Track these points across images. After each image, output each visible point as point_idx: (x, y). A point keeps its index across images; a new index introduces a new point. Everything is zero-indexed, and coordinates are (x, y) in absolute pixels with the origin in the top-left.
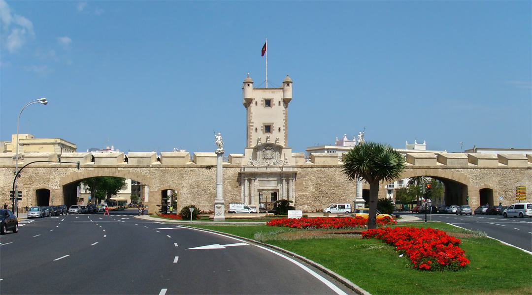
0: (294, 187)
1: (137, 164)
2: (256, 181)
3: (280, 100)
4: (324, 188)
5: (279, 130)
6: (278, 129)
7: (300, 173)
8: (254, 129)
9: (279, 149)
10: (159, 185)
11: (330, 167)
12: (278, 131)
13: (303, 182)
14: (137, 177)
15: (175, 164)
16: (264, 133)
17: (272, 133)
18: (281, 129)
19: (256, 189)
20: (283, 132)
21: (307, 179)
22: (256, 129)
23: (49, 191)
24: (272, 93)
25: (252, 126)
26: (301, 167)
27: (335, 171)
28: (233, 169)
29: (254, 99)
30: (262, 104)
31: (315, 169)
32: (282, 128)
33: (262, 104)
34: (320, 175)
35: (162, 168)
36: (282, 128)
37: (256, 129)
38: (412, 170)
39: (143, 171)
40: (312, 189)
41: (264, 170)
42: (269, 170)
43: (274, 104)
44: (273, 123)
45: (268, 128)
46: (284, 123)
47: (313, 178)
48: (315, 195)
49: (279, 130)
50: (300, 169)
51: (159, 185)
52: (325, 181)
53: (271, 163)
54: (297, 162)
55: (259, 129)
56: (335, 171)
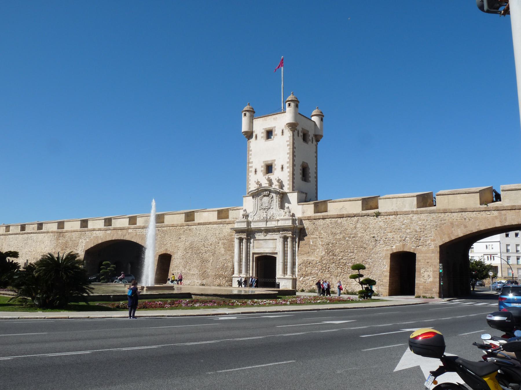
4: (338, 250)
6: (281, 167)
8: (253, 170)
12: (281, 169)
15: (175, 223)
16: (264, 175)
18: (284, 167)
22: (256, 171)
23: (441, 247)
25: (252, 167)
30: (262, 137)
31: (328, 221)
34: (334, 230)
35: (164, 228)
37: (256, 171)
40: (321, 252)
42: (272, 224)
43: (276, 135)
44: (275, 160)
45: (269, 168)
47: (324, 235)
54: (303, 213)
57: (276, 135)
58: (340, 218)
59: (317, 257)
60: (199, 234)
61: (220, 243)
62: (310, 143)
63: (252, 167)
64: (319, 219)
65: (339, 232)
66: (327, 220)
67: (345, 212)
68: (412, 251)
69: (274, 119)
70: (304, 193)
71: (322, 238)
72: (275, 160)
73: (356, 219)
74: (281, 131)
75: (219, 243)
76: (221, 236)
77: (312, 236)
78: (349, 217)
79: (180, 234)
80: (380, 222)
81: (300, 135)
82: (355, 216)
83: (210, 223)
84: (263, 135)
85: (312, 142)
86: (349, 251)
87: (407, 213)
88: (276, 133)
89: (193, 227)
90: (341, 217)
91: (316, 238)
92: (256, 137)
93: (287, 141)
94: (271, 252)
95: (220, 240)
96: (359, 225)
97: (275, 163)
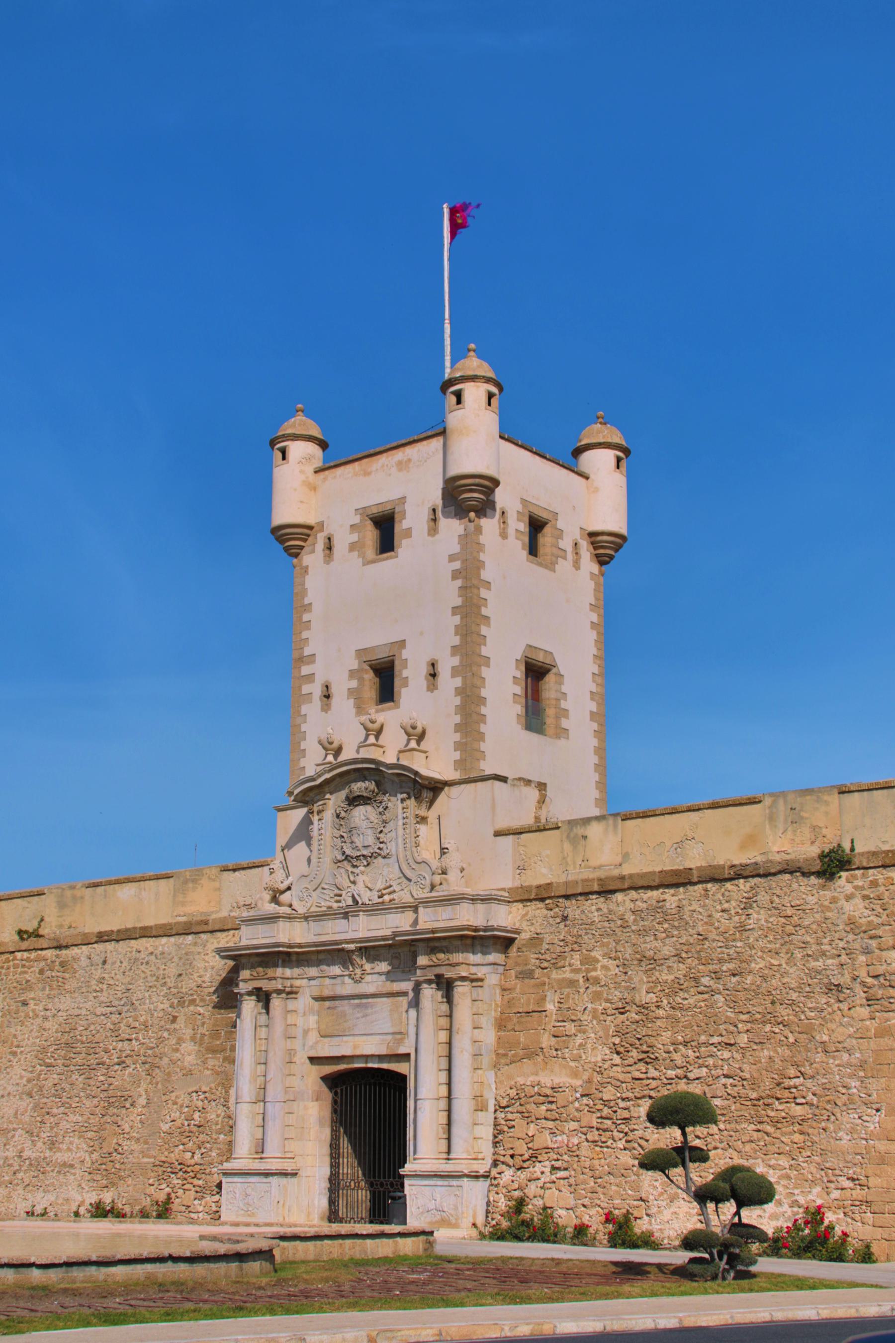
0: (489, 1036)
2: (304, 1001)
4: (666, 1036)
6: (424, 670)
7: (536, 940)
8: (316, 689)
9: (427, 790)
11: (715, 877)
13: (544, 998)
19: (301, 1058)
20: (448, 683)
21: (567, 974)
24: (402, 466)
25: (310, 678)
26: (541, 895)
27: (748, 904)
29: (321, 524)
30: (353, 547)
32: (447, 663)
34: (649, 945)
41: (336, 931)
43: (408, 533)
44: (402, 644)
45: (385, 678)
46: (458, 629)
47: (606, 968)
48: (609, 1093)
50: (537, 910)
52: (677, 987)
53: (367, 884)
54: (521, 869)
55: (342, 686)
56: (748, 904)
58: (677, 885)
59: (575, 1074)
60: (101, 980)
61: (181, 1020)
62: (564, 566)
63: (310, 678)
64: (586, 894)
65: (667, 951)
66: (619, 896)
67: (694, 859)
69: (400, 463)
70: (528, 782)
71: (597, 981)
72: (402, 644)
74: (425, 515)
75: (174, 1019)
76: (188, 985)
77: (555, 975)
78: (713, 880)
79: (28, 986)
80: (849, 898)
81: (511, 531)
82: (738, 876)
83: (145, 933)
85: (577, 565)
86: (715, 1039)
88: (405, 524)
89: (75, 951)
90: (679, 880)
91: (572, 983)
92: (329, 548)
93: (452, 558)
94: (383, 1051)
95: (181, 1003)
96: (758, 917)
97: (405, 654)
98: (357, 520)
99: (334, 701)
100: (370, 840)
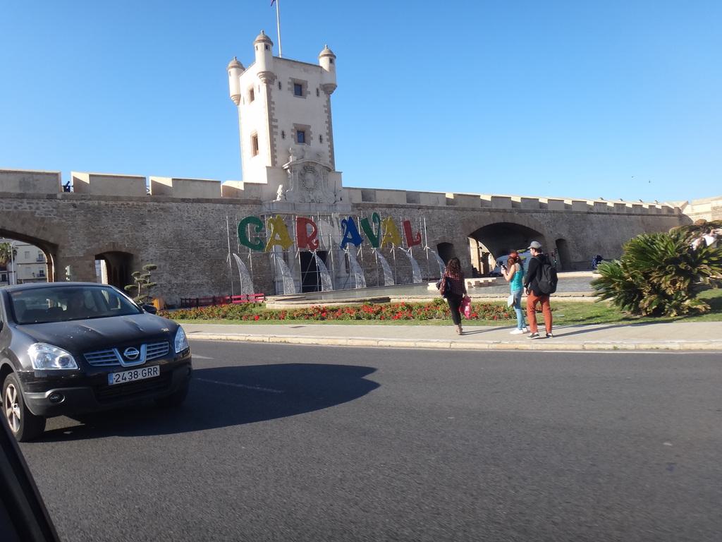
1: (18, 191)
3: (318, 86)
5: (321, 139)
10: (85, 243)
14: (23, 223)
16: (296, 143)
17: (309, 144)
22: (283, 134)
24: (305, 70)
28: (247, 208)
30: (289, 89)
32: (325, 137)
33: (289, 89)
35: (90, 203)
36: (325, 137)
37: (283, 134)
38: (489, 214)
39: (38, 209)
43: (309, 93)
44: (309, 127)
49: (321, 139)
51: (85, 243)
57: (309, 93)
68: (450, 242)
73: (403, 210)
74: (315, 90)
78: (396, 208)
83: (208, 201)
84: (289, 86)
87: (440, 208)
89: (168, 204)
98: (290, 81)
99: (286, 137)
100: (313, 184)
